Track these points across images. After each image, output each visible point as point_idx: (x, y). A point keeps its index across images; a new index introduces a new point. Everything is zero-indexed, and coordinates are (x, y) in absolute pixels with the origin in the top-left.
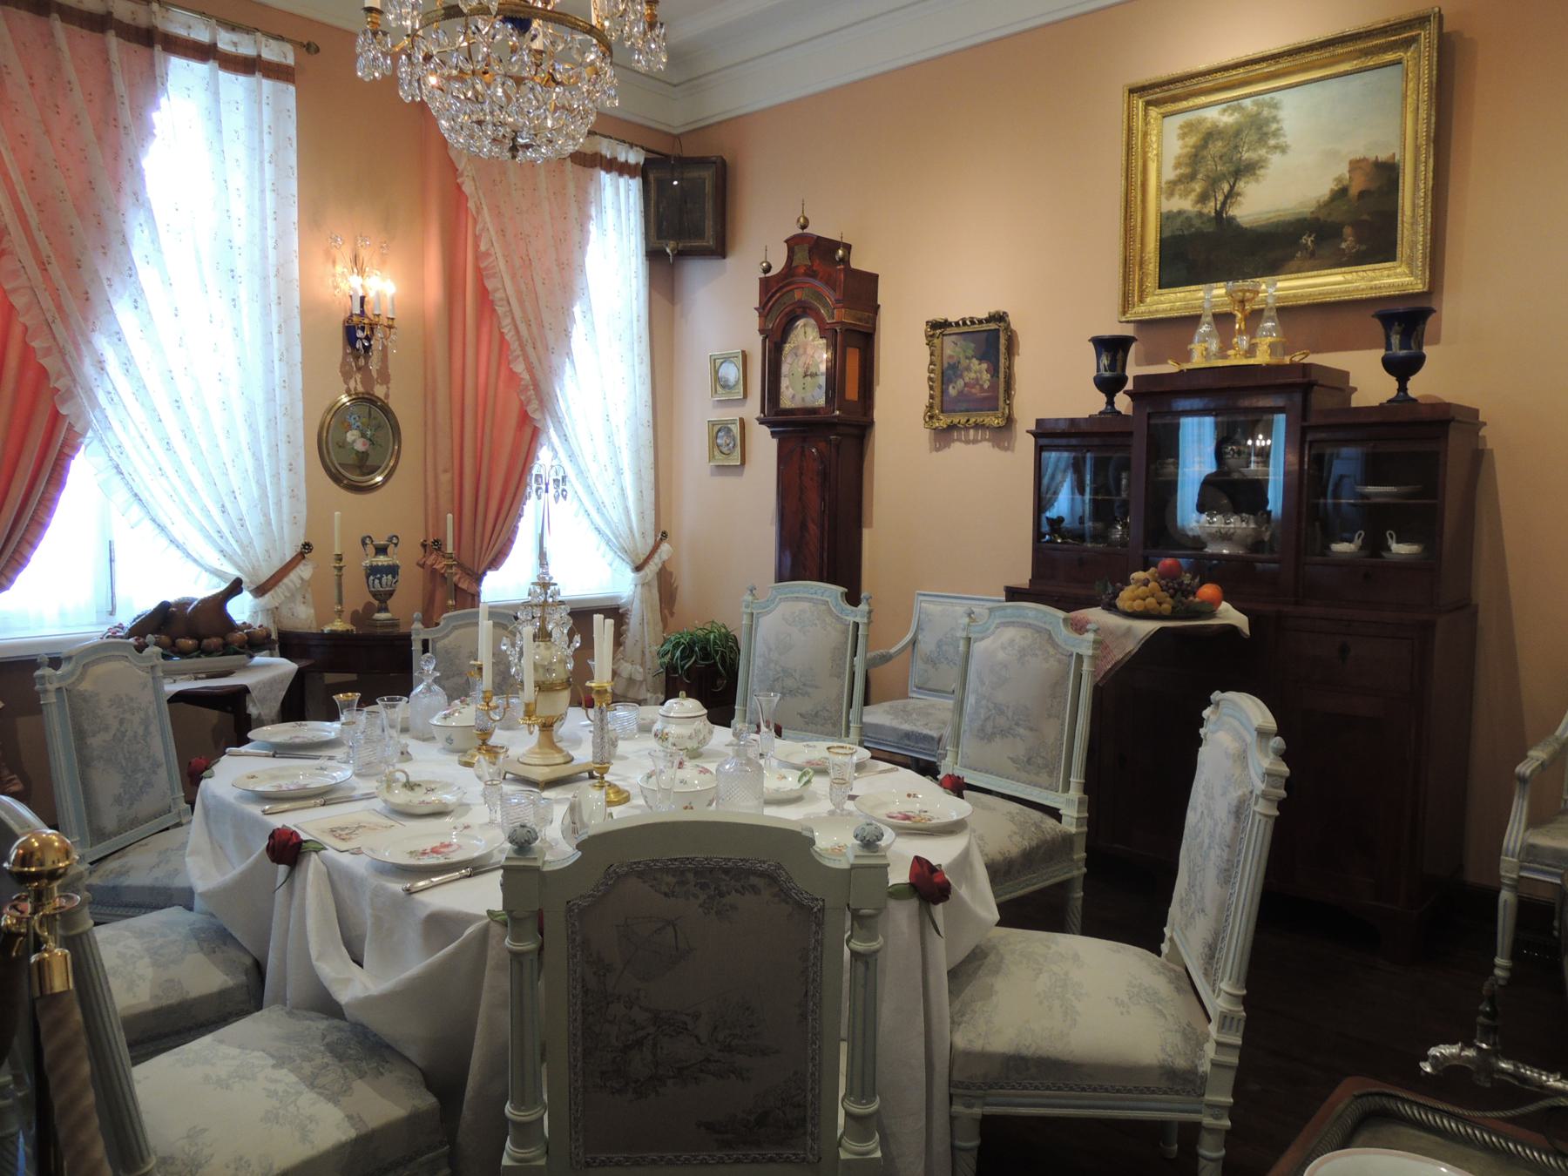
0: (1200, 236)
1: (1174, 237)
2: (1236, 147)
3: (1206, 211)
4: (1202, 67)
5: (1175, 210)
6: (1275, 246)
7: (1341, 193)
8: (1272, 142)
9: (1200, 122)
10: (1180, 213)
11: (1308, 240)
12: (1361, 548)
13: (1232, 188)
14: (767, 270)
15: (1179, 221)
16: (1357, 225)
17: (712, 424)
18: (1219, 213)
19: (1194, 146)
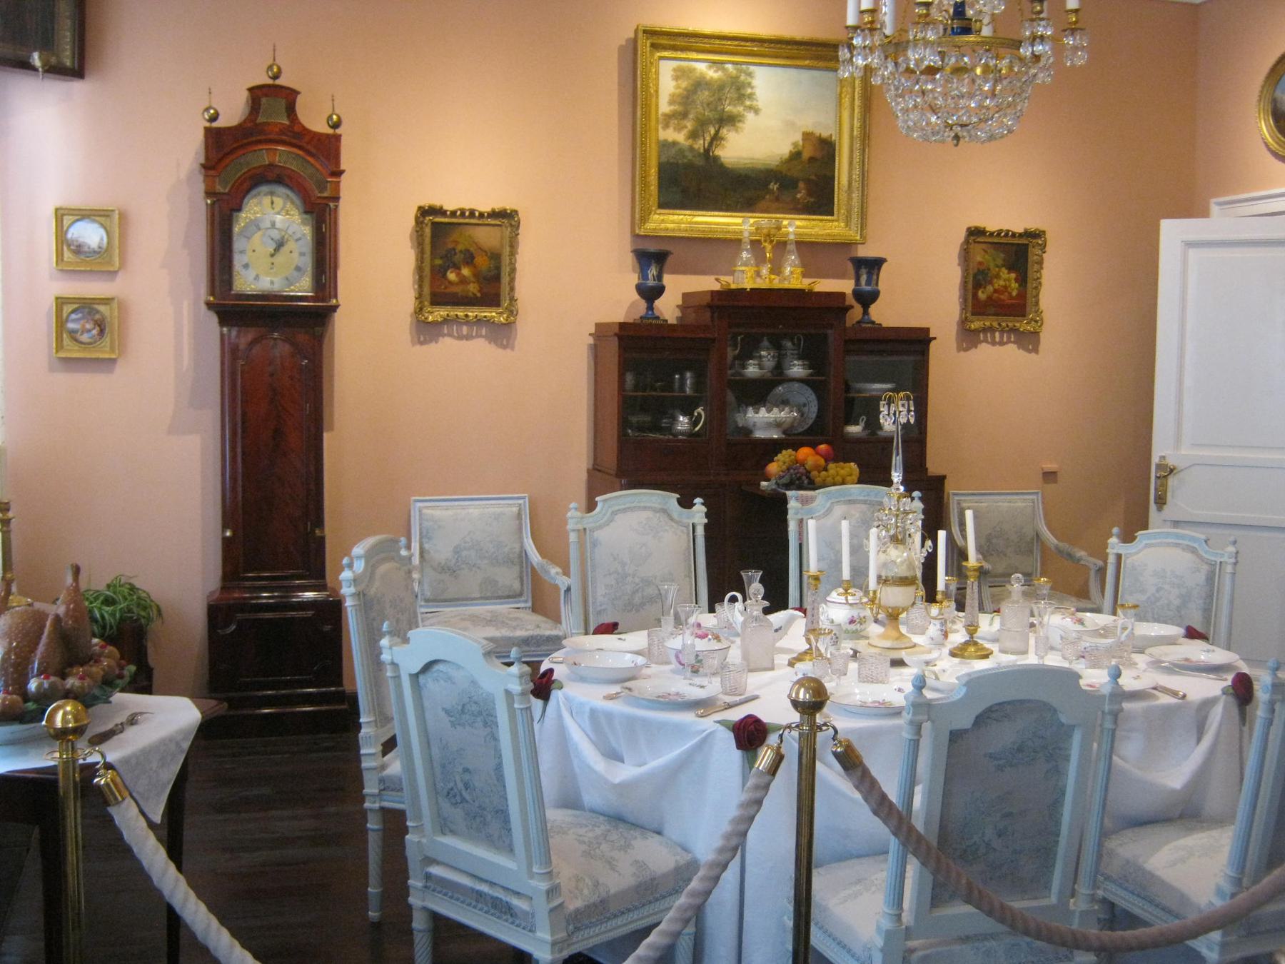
0: (690, 166)
1: (668, 163)
2: (720, 99)
3: (696, 147)
4: (707, 28)
5: (670, 140)
6: (744, 188)
7: (796, 156)
8: (748, 103)
9: (692, 70)
10: (675, 143)
11: (774, 187)
12: (864, 429)
13: (717, 132)
14: (214, 118)
15: (673, 151)
16: (808, 181)
17: (61, 302)
18: (707, 151)
19: (685, 89)
